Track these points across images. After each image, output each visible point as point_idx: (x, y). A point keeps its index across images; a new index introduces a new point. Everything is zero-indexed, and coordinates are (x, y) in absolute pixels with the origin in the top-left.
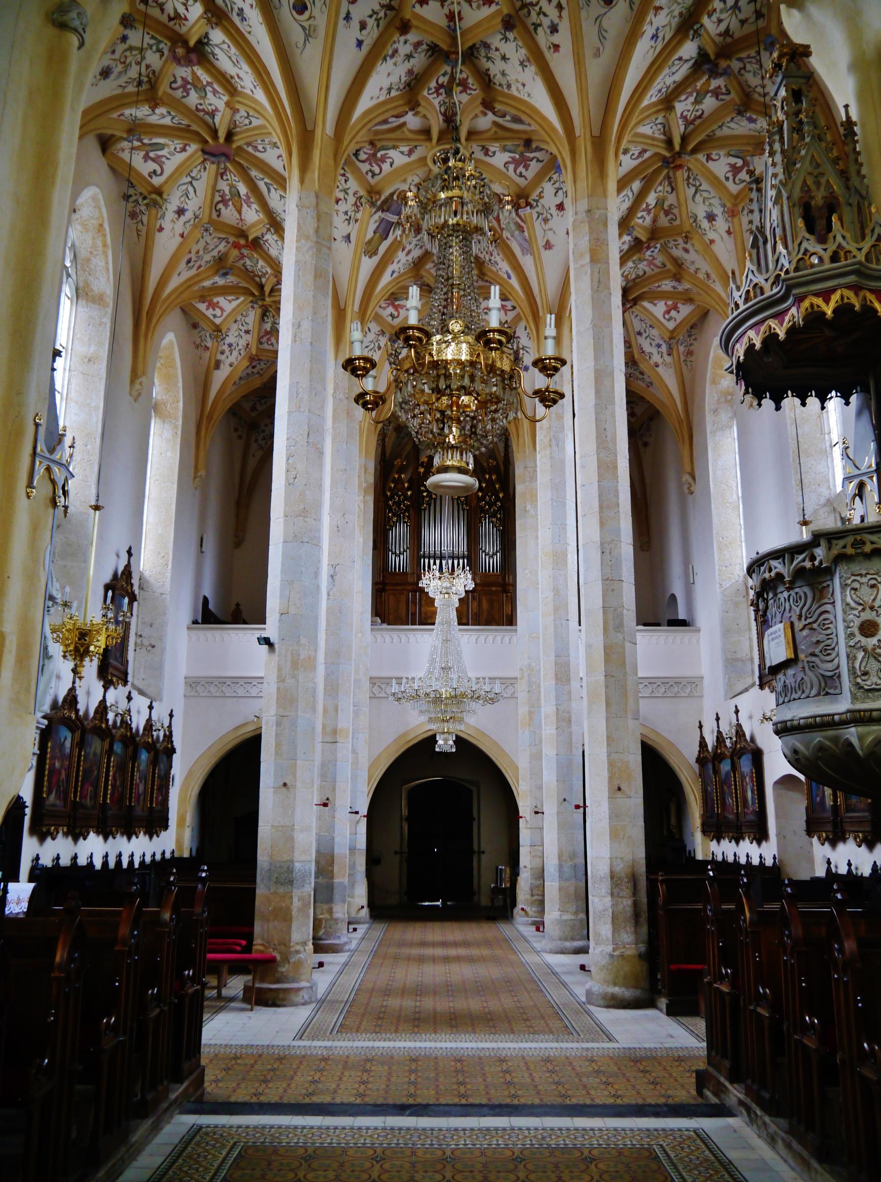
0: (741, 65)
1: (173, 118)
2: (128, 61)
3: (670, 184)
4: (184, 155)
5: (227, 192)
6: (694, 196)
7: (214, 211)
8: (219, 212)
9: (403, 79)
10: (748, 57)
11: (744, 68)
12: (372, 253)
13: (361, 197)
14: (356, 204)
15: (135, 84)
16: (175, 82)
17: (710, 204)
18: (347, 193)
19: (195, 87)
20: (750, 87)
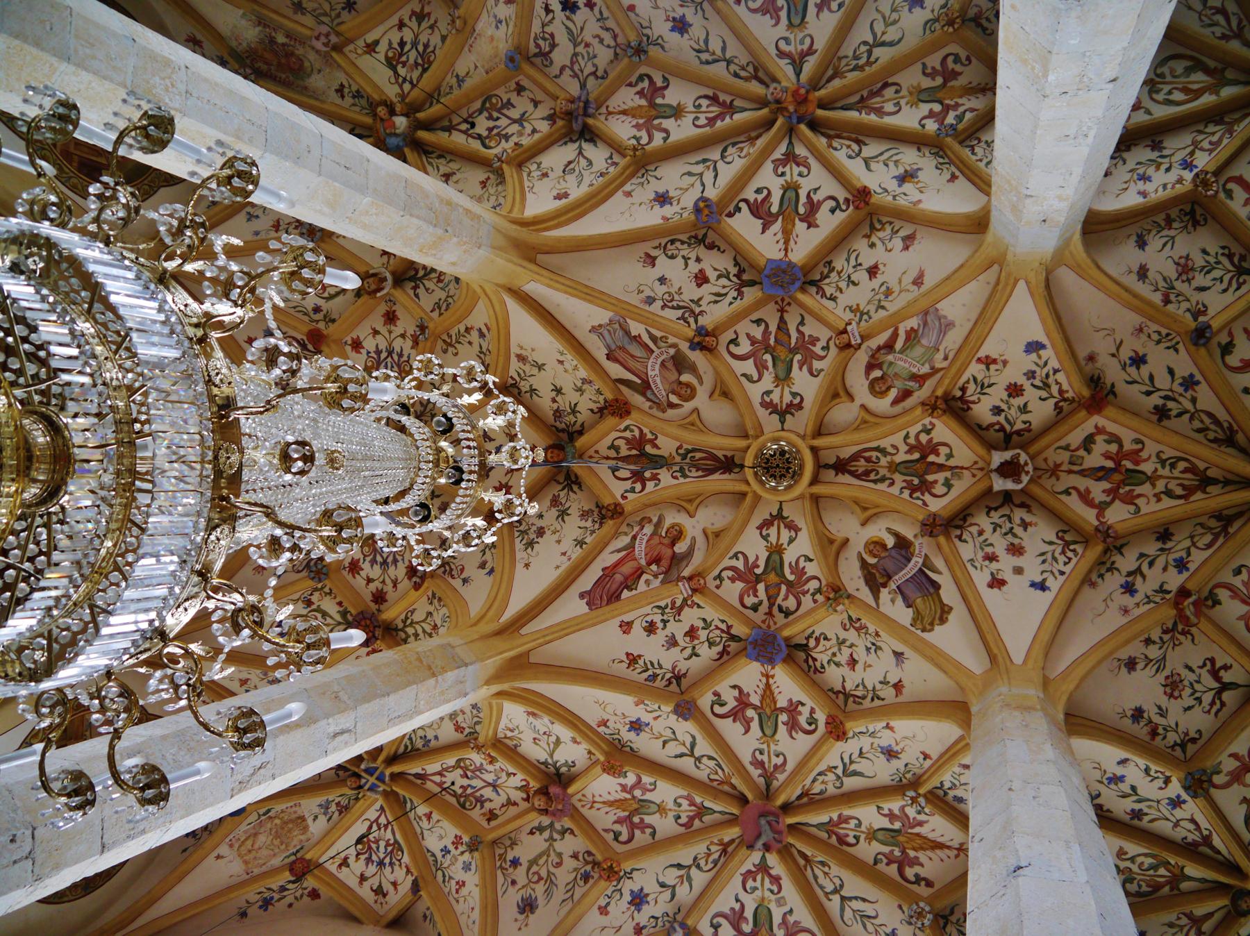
0: (591, 82)
1: (698, 867)
2: (544, 873)
3: (878, 93)
4: (786, 883)
5: (886, 849)
6: (891, 44)
7: (914, 887)
8: (918, 879)
9: (589, 524)
10: (575, 76)
11: (594, 74)
12: (944, 613)
13: (850, 618)
14: (857, 629)
15: (581, 883)
16: (617, 836)
17: (894, 10)
18: (844, 641)
19: (636, 812)
20: (616, 54)
